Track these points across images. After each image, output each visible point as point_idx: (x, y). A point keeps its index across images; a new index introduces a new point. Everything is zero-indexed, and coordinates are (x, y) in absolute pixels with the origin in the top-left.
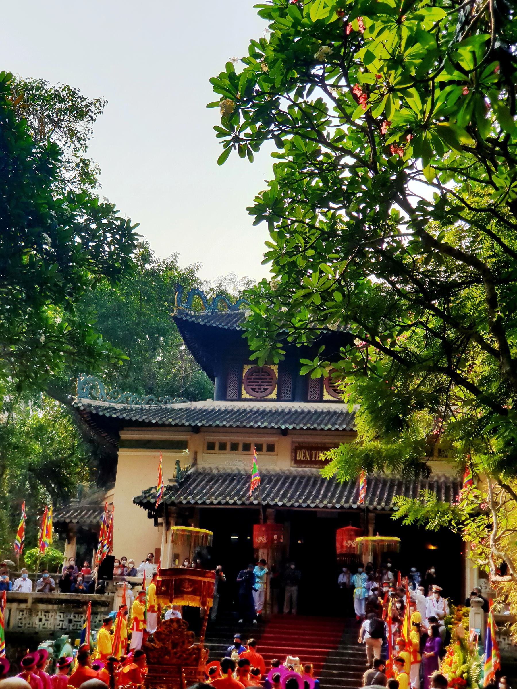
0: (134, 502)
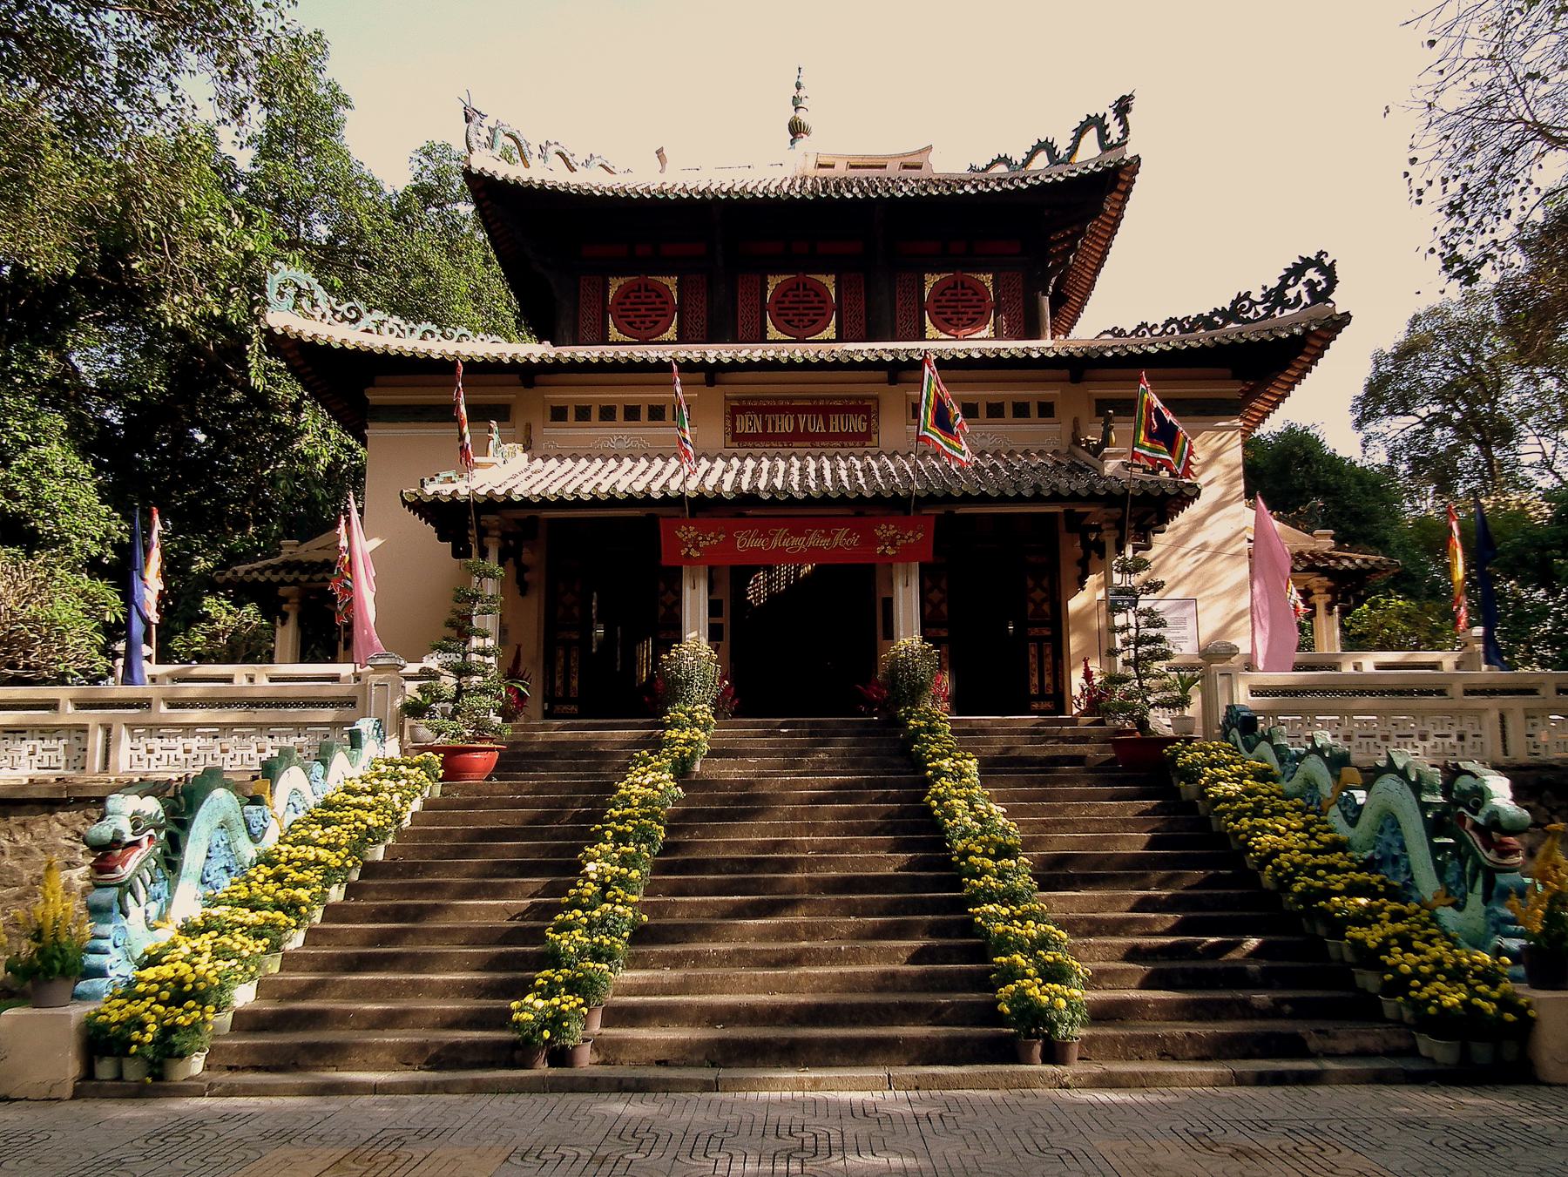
0: (405, 503)
